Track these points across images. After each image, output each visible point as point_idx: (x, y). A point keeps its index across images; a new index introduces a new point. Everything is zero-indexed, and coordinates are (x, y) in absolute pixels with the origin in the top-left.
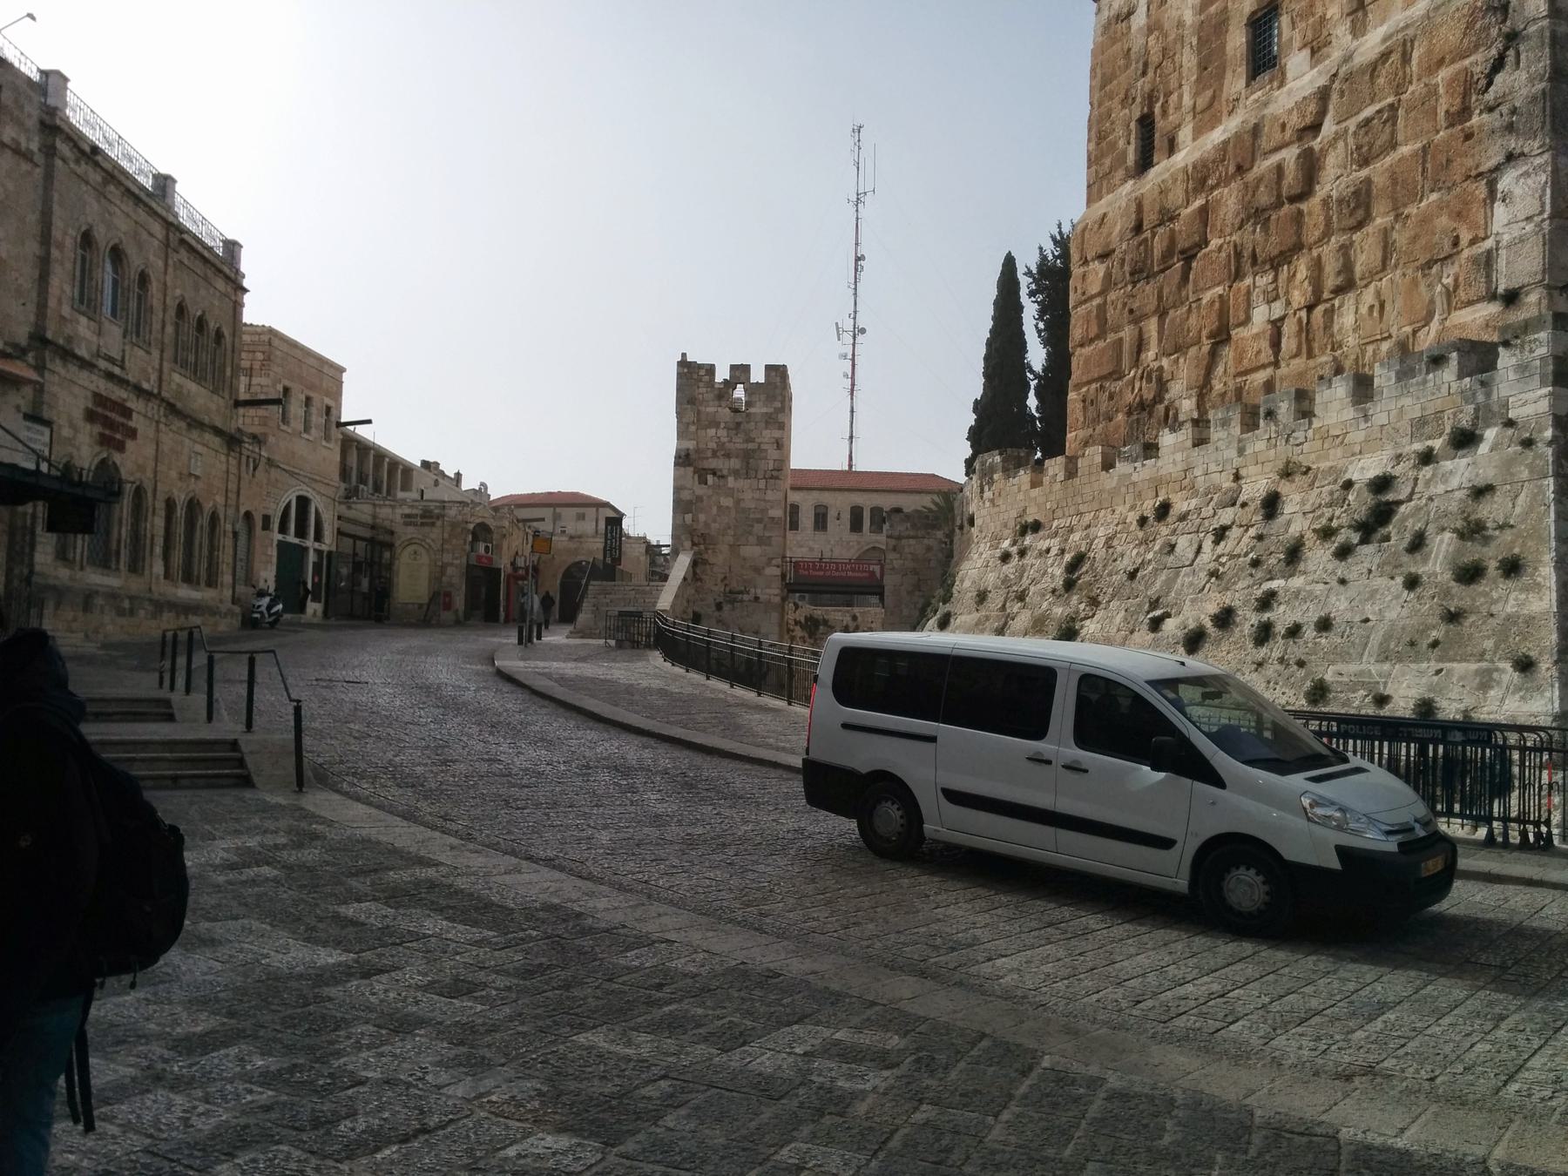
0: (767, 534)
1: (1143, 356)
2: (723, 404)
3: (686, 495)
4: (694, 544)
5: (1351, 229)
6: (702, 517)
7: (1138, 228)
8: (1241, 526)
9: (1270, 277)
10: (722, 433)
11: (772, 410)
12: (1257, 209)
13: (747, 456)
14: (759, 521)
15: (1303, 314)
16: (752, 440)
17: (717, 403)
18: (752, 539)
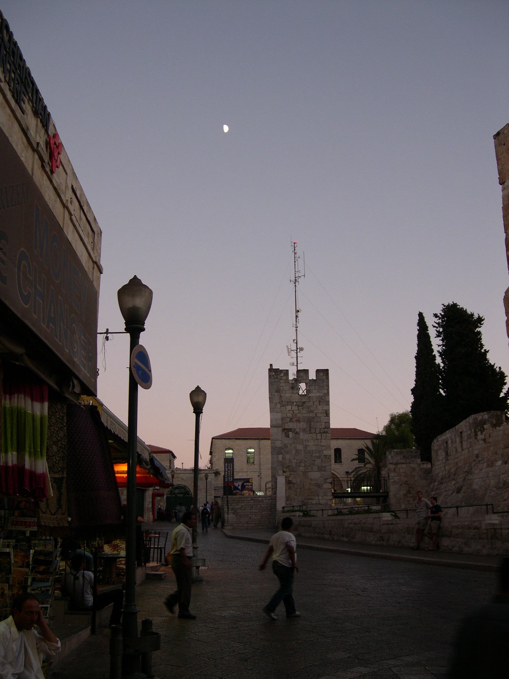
4: (284, 472)
6: (288, 457)
10: (295, 408)
11: (321, 395)
17: (291, 391)
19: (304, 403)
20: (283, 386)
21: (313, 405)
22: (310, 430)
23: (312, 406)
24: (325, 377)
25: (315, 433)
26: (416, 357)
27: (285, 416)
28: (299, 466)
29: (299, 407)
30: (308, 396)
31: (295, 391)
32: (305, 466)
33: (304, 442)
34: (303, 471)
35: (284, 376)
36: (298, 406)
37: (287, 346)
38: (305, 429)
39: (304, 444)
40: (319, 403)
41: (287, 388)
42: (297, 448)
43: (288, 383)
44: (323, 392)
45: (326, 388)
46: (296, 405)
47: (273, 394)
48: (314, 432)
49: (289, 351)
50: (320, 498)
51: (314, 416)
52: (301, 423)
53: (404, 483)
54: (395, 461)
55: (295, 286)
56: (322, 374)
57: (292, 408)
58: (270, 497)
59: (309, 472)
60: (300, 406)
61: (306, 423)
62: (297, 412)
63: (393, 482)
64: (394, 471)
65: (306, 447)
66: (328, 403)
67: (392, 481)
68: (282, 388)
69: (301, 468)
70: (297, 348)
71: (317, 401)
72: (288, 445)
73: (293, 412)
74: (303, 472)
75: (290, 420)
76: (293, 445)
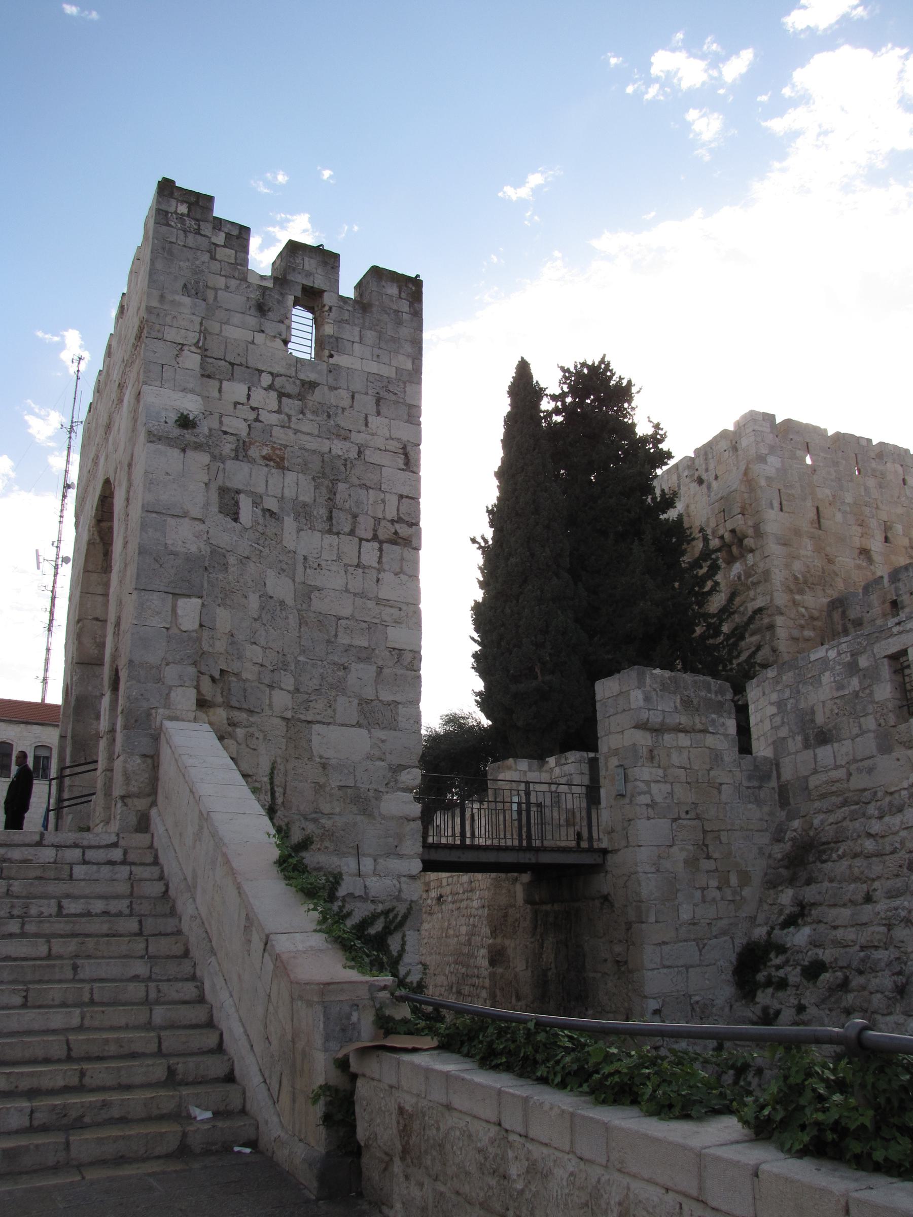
0: (386, 696)
6: (224, 619)
10: (265, 400)
11: (387, 372)
14: (365, 655)
17: (252, 321)
18: (346, 708)
19: (312, 385)
20: (216, 290)
21: (352, 407)
22: (330, 518)
23: (343, 409)
24: (405, 306)
26: (500, 474)
27: (216, 425)
28: (271, 687)
29: (284, 399)
30: (331, 361)
31: (271, 327)
32: (297, 690)
33: (300, 568)
34: (289, 715)
35: (225, 246)
36: (281, 395)
37: (37, 551)
38: (305, 505)
39: (297, 580)
40: (378, 401)
41: (235, 300)
43: (244, 279)
45: (408, 348)
46: (271, 387)
47: (169, 297)
50: (367, 864)
51: (353, 454)
52: (291, 477)
53: (687, 812)
54: (656, 718)
55: (70, 438)
57: (249, 397)
58: (115, 845)
59: (316, 727)
60: (289, 396)
61: (314, 479)
62: (274, 418)
63: (647, 805)
64: (652, 758)
65: (307, 593)
66: (412, 415)
67: (645, 799)
69: (281, 700)
70: (57, 558)
71: (367, 394)
72: (232, 560)
73: (253, 416)
74: (284, 718)
75: (236, 450)
76: (252, 567)
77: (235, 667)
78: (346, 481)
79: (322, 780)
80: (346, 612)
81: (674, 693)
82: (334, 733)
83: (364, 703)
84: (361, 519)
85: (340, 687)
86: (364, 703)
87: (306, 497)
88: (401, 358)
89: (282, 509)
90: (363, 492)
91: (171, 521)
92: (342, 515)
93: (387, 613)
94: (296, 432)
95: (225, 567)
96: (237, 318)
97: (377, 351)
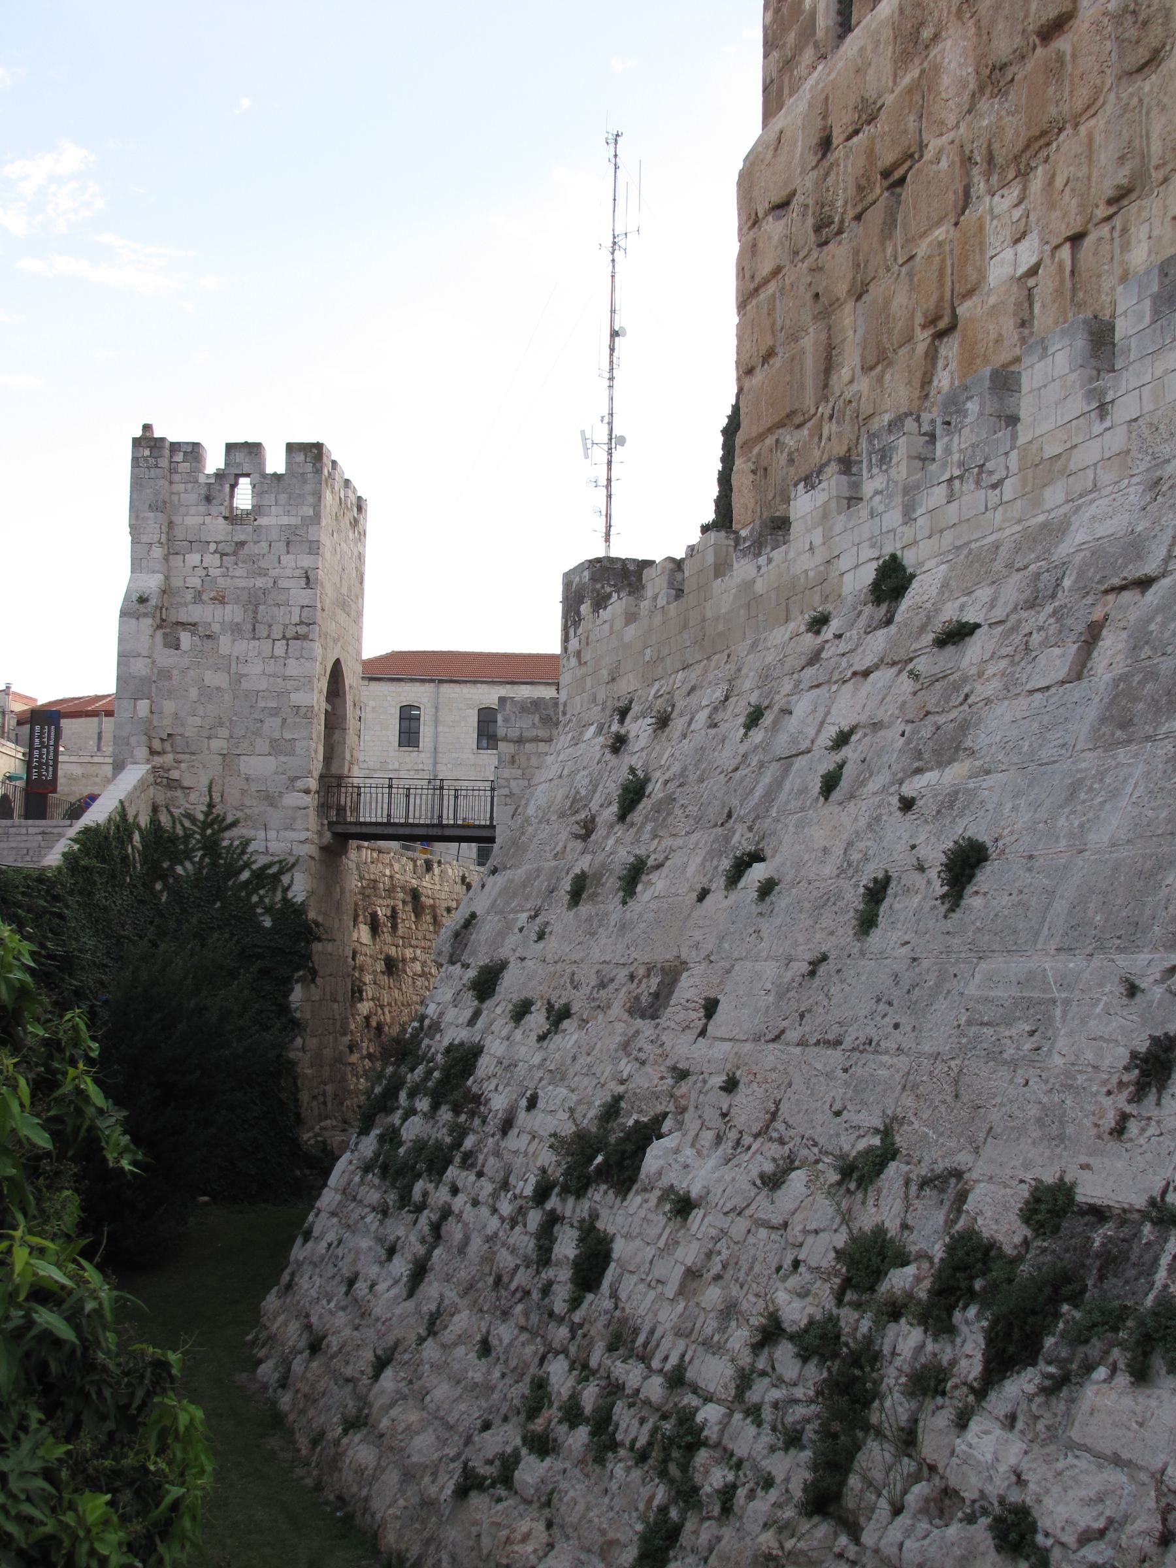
0: (288, 736)
1: (834, 378)
2: (215, 510)
3: (140, 667)
4: (153, 752)
5: (1140, 69)
6: (169, 707)
7: (826, 144)
8: (894, 664)
9: (1014, 192)
10: (212, 560)
11: (294, 521)
12: (994, 67)
13: (254, 602)
14: (275, 712)
15: (1065, 252)
16: (263, 573)
17: (202, 509)
18: (262, 745)
20: (179, 494)
22: (254, 630)
24: (309, 468)
25: (268, 637)
28: (209, 738)
32: (231, 737)
33: (234, 665)
36: (223, 555)
37: (583, 432)
38: (237, 624)
40: (288, 544)
41: (192, 497)
42: (207, 683)
44: (300, 513)
46: (215, 552)
47: (142, 515)
48: (265, 635)
49: (587, 444)
50: (272, 834)
51: (271, 584)
52: (228, 607)
56: (300, 458)
59: (242, 757)
62: (218, 572)
68: (175, 498)
69: (217, 744)
70: (610, 439)
72: (175, 672)
73: (204, 573)
75: (194, 597)
77: (179, 730)
78: (265, 603)
79: (246, 788)
80: (264, 687)
81: (533, 713)
82: (254, 760)
83: (273, 742)
84: (274, 627)
85: (258, 733)
86: (273, 742)
87: (238, 619)
88: (305, 508)
89: (223, 629)
90: (276, 609)
91: (132, 659)
92: (262, 626)
93: (290, 685)
94: (233, 577)
95: (170, 678)
96: (193, 510)
97: (288, 508)
